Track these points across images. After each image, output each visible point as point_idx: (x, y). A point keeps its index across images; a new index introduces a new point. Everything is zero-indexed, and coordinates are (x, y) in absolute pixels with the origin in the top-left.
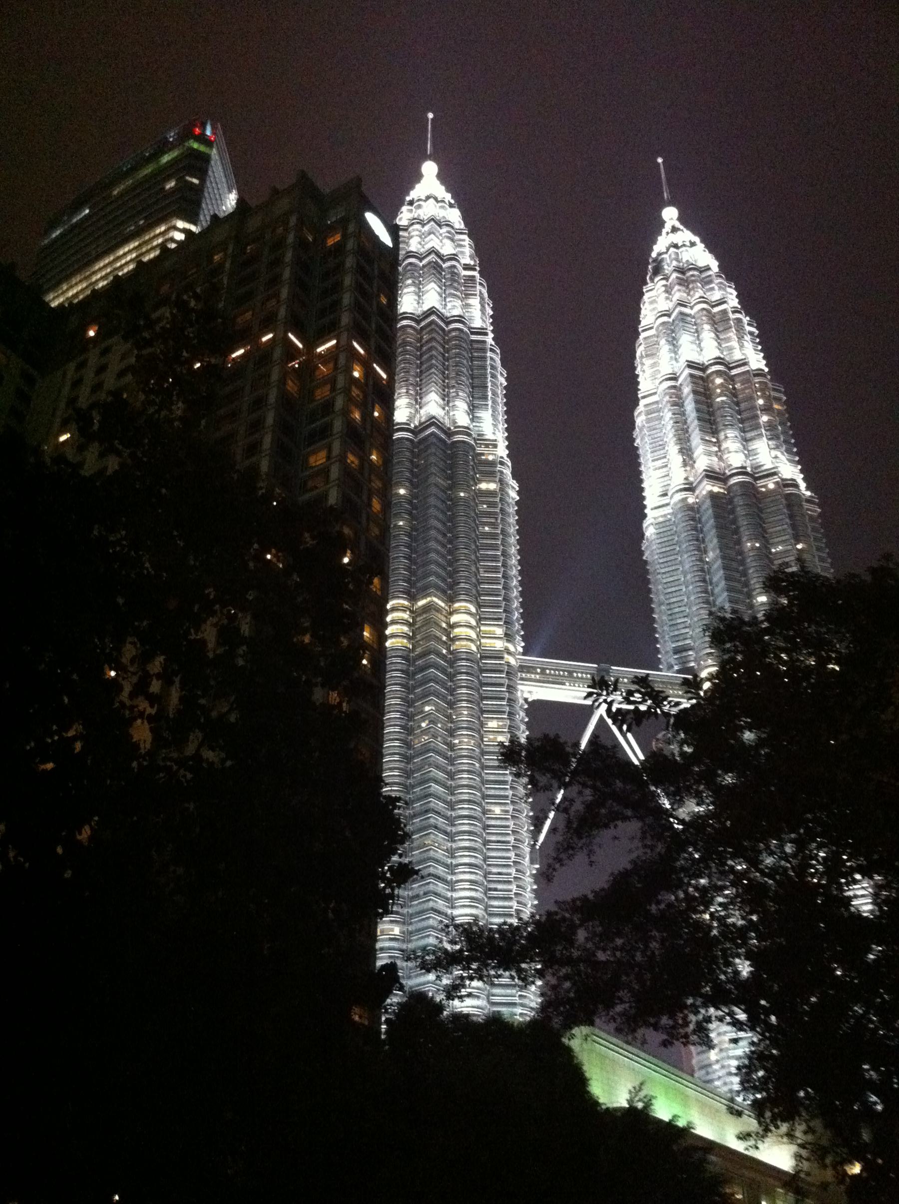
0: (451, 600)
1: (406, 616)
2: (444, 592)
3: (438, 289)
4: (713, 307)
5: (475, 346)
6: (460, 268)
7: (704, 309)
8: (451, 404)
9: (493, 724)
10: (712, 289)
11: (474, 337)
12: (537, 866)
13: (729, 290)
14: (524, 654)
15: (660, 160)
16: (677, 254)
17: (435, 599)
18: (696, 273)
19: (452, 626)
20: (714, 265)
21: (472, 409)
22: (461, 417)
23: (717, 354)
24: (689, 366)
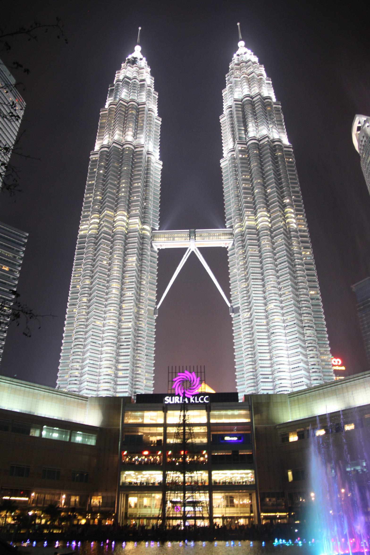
0: (116, 211)
1: (98, 221)
2: (112, 208)
3: (127, 91)
4: (249, 75)
5: (140, 110)
6: (137, 81)
7: (244, 77)
8: (126, 134)
9: (130, 259)
10: (250, 68)
11: (140, 107)
12: (157, 316)
13: (260, 68)
14: (159, 230)
15: (238, 24)
16: (239, 58)
17: (108, 212)
18: (244, 64)
19: (114, 222)
20: (255, 59)
21: (135, 135)
22: (129, 138)
23: (249, 93)
24: (235, 101)
